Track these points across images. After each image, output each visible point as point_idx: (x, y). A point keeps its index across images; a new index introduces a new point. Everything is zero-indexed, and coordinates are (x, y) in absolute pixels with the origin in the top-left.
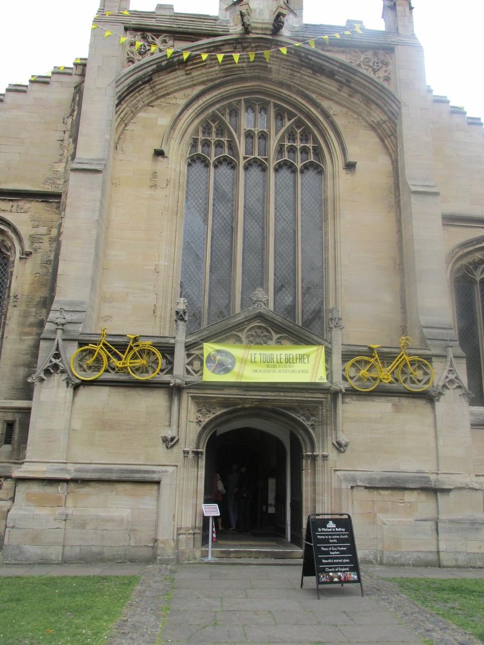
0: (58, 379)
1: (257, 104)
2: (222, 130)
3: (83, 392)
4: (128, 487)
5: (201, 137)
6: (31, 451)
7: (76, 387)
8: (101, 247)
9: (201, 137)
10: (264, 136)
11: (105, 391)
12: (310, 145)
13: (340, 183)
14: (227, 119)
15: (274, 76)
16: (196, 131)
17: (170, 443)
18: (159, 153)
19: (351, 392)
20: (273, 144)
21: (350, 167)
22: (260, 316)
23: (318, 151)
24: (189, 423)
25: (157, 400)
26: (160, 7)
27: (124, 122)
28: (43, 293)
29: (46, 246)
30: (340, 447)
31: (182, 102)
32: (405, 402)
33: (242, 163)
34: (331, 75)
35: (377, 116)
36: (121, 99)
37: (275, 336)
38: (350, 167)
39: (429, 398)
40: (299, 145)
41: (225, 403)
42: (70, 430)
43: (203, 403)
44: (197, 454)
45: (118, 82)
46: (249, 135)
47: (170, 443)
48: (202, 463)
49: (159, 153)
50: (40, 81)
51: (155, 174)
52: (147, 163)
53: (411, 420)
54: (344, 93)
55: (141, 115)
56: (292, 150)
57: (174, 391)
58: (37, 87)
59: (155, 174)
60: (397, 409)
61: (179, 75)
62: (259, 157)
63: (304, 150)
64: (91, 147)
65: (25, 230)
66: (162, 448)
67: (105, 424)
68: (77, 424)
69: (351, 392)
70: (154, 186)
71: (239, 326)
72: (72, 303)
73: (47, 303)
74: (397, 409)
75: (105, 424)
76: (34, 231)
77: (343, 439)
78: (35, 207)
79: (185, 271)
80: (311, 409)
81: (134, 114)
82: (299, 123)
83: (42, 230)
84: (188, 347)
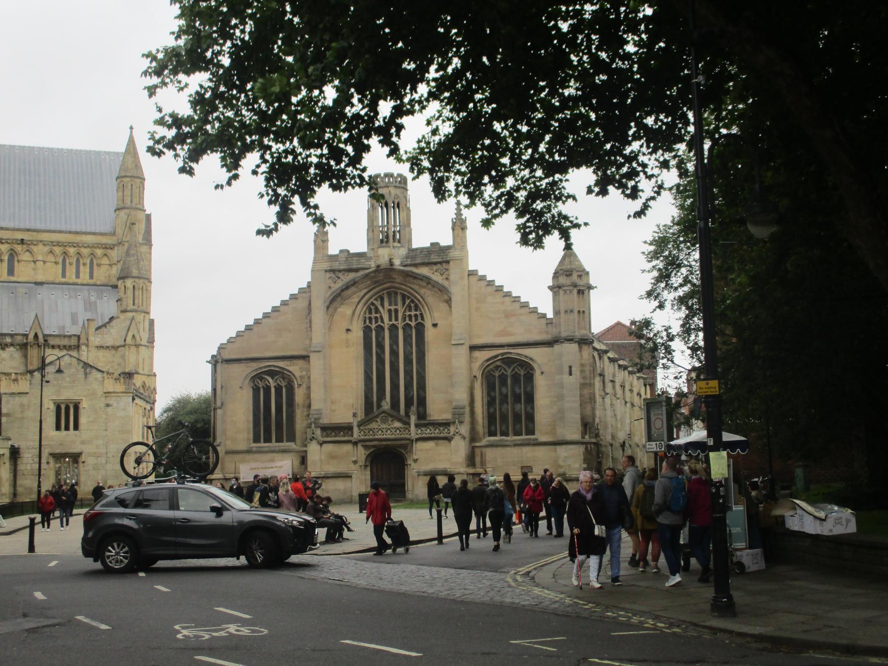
0: (314, 442)
1: (392, 294)
2: (377, 311)
3: (325, 446)
4: (341, 479)
5: (368, 315)
6: (309, 469)
7: (321, 445)
8: (327, 387)
9: (368, 315)
10: (396, 311)
11: (331, 445)
12: (418, 313)
13: (430, 334)
14: (378, 303)
15: (398, 280)
16: (365, 313)
17: (355, 462)
18: (348, 330)
19: (418, 440)
20: (400, 315)
21: (435, 325)
22: (384, 412)
23: (421, 314)
24: (361, 453)
25: (349, 447)
26: (341, 251)
27: (332, 316)
28: (307, 402)
29: (306, 379)
30: (415, 461)
31: (357, 300)
32: (440, 441)
33: (386, 327)
34: (421, 280)
35: (446, 297)
36: (328, 308)
37: (390, 419)
38: (435, 325)
39: (448, 439)
40: (413, 313)
41: (374, 446)
42: (321, 461)
43: (366, 447)
44: (366, 466)
45: (325, 302)
46: (390, 311)
47: (355, 462)
48: (369, 468)
49: (348, 330)
50: (293, 297)
51: (347, 340)
52: (344, 335)
53: (442, 449)
54: (430, 286)
55: (339, 310)
56: (410, 316)
57: (355, 444)
58: (293, 301)
59: (347, 340)
60: (437, 445)
61: (353, 289)
62: (394, 322)
63: (416, 316)
64: (318, 336)
65: (297, 374)
66: (352, 465)
67: (332, 457)
68: (323, 458)
69: (418, 440)
70: (348, 347)
71: (377, 416)
72: (318, 410)
73: (309, 406)
74: (437, 445)
75: (332, 457)
76: (301, 374)
77: (415, 457)
78: (301, 362)
79: (366, 385)
80: (405, 447)
81: (335, 310)
82: (412, 301)
83: (304, 373)
84: (359, 426)
